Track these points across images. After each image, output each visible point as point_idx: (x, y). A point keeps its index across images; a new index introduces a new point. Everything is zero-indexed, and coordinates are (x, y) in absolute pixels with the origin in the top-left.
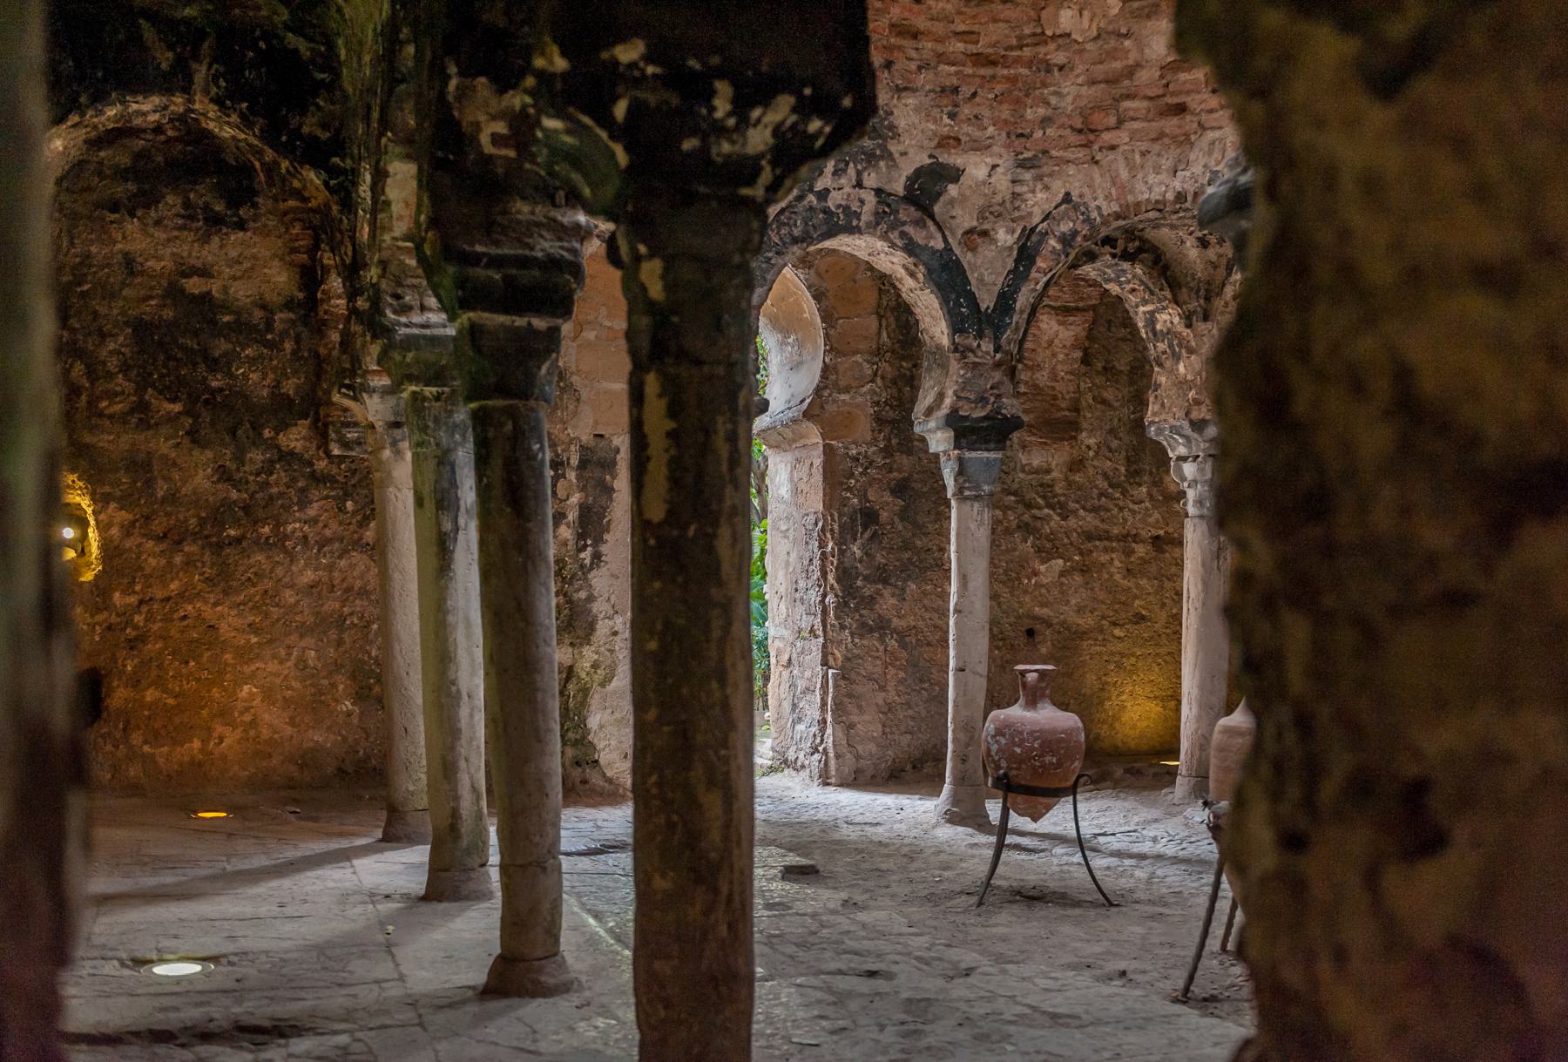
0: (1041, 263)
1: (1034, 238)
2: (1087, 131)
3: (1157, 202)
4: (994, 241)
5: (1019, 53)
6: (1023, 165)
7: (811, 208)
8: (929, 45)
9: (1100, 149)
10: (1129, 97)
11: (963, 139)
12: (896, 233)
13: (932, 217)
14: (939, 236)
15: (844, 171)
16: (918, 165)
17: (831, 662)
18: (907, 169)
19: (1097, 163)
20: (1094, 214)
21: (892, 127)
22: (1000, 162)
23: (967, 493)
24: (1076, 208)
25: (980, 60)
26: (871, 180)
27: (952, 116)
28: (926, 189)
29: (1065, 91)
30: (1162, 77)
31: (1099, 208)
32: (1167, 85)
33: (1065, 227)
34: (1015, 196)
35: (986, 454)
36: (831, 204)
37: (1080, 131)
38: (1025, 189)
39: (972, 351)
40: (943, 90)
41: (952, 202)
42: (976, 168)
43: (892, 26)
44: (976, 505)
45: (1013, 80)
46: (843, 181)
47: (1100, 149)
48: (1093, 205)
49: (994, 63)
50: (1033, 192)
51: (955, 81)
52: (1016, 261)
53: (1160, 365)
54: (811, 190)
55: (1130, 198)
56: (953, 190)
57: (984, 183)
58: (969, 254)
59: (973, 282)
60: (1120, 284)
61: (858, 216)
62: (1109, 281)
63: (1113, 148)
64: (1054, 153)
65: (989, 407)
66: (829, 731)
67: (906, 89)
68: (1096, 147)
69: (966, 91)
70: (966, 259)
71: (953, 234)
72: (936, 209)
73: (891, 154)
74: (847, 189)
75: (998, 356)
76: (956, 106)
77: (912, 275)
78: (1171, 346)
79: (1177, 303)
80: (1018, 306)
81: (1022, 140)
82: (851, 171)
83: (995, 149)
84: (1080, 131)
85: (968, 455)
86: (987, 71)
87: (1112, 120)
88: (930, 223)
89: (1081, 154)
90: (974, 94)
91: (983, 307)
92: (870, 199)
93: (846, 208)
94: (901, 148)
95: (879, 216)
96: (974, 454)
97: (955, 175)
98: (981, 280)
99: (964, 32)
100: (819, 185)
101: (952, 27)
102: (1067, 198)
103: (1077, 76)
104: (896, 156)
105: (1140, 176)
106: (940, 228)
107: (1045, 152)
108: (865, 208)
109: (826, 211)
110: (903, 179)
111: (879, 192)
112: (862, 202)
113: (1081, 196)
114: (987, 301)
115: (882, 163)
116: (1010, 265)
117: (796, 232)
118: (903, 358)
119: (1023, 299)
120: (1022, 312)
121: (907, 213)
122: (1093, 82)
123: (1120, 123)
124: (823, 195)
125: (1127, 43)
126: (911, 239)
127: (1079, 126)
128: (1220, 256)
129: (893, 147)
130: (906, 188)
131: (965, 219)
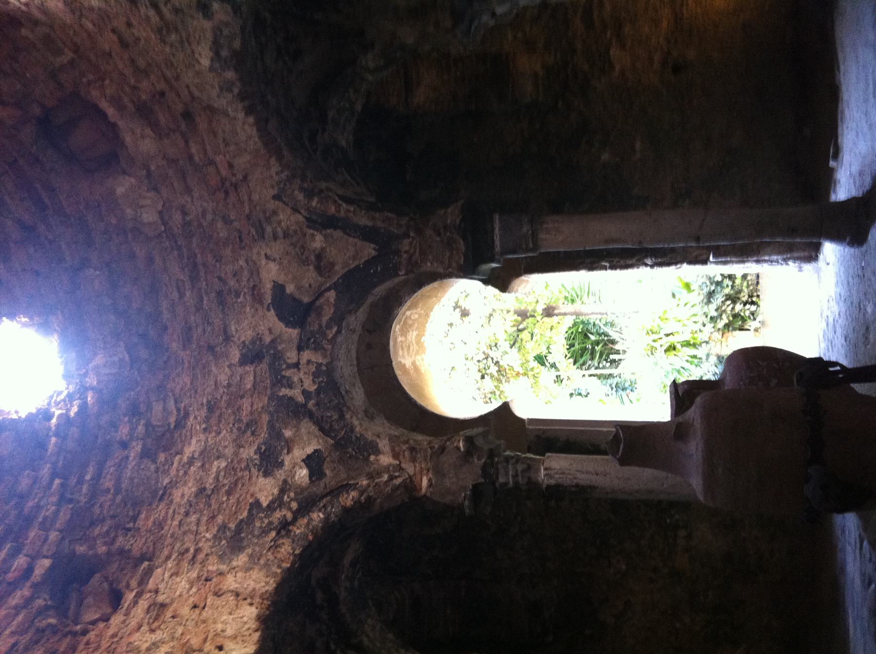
0: (333, 210)
1: (314, 217)
3: (258, 130)
4: (323, 249)
6: (262, 235)
7: (317, 404)
8: (192, 318)
9: (234, 175)
10: (191, 158)
12: (328, 332)
13: (313, 302)
14: (328, 294)
15: (289, 379)
16: (276, 319)
17: (704, 257)
18: (280, 327)
19: (245, 178)
20: (283, 176)
21: (253, 342)
22: (263, 253)
23: (531, 245)
26: (292, 356)
27: (237, 295)
29: (200, 210)
34: (286, 235)
35: (497, 231)
37: (227, 193)
38: (279, 229)
39: (411, 257)
41: (299, 288)
43: (184, 348)
44: (542, 236)
46: (296, 379)
47: (234, 175)
48: (276, 178)
49: (195, 265)
50: (279, 222)
52: (335, 228)
54: (305, 406)
55: (262, 152)
56: (290, 289)
57: (280, 264)
58: (337, 268)
59: (357, 263)
61: (319, 365)
63: (231, 166)
64: (247, 211)
65: (455, 236)
66: (767, 258)
67: (225, 332)
68: (234, 180)
70: (340, 270)
71: (322, 284)
72: (306, 300)
74: (301, 375)
75: (412, 234)
80: (369, 223)
82: (288, 373)
83: (255, 257)
84: (227, 193)
85: (498, 249)
87: (211, 169)
88: (318, 303)
89: (243, 191)
90: (220, 278)
91: (374, 253)
92: (306, 355)
94: (267, 332)
95: (317, 348)
96: (497, 242)
98: (354, 258)
99: (179, 291)
100: (301, 399)
101: (177, 300)
102: (276, 197)
103: (187, 202)
106: (320, 295)
108: (314, 359)
109: (318, 392)
110: (287, 329)
111: (300, 349)
112: (309, 362)
113: (272, 187)
114: (370, 250)
115: (280, 348)
116: (338, 234)
117: (335, 417)
119: (363, 220)
120: (373, 219)
122: (188, 190)
123: (212, 162)
124: (305, 393)
125: (153, 168)
126: (331, 319)
127: (223, 195)
129: (267, 339)
130: (294, 327)
131: (310, 276)
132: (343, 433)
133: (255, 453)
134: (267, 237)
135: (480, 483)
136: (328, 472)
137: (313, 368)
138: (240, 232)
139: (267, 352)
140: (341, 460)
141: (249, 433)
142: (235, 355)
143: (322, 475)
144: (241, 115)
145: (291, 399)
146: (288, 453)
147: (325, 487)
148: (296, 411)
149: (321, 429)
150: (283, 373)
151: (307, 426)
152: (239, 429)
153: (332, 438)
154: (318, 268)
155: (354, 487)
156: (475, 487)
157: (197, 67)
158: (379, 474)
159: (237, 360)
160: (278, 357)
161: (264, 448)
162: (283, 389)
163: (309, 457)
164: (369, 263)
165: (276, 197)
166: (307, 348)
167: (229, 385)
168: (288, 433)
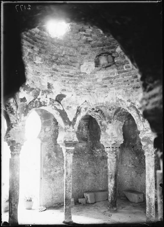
1: (80, 108)
2: (89, 89)
5: (76, 75)
6: (77, 95)
7: (37, 101)
9: (92, 93)
11: (66, 89)
13: (60, 104)
14: (62, 107)
15: (43, 95)
21: (53, 87)
24: (87, 103)
25: (69, 76)
26: (49, 96)
27: (64, 85)
28: (59, 98)
30: (102, 81)
31: (92, 103)
32: (103, 82)
33: (85, 106)
34: (76, 101)
36: (41, 101)
40: (63, 81)
41: (64, 101)
42: (68, 95)
45: (75, 80)
48: (90, 103)
49: (72, 77)
51: (65, 80)
53: (102, 130)
54: (37, 98)
55: (97, 102)
56: (64, 99)
60: (95, 116)
62: (93, 116)
68: (91, 92)
69: (67, 81)
72: (61, 102)
73: (52, 92)
74: (44, 98)
76: (65, 84)
77: (57, 114)
78: (104, 127)
79: (105, 120)
81: (77, 90)
83: (73, 92)
86: (71, 78)
88: (60, 105)
92: (49, 100)
93: (44, 102)
94: (55, 91)
97: (64, 96)
102: (86, 101)
104: (53, 92)
105: (99, 98)
106: (62, 106)
107: (82, 93)
108: (48, 102)
109: (39, 102)
111: (50, 99)
112: (47, 101)
114: (71, 120)
115: (51, 94)
116: (76, 113)
117: (34, 106)
118: (56, 127)
121: (56, 103)
126: (56, 108)
128: (113, 112)
129: (53, 90)
130: (56, 98)
132: (30, 107)
133: (27, 84)
134: (77, 96)
135: (15, 143)
136: (21, 103)
137: (46, 101)
138: (78, 90)
139: (50, 90)
140: (23, 107)
141: (32, 83)
142: (50, 82)
143: (21, 101)
144: (106, 100)
145: (39, 95)
146: (27, 93)
147: (18, 102)
148: (36, 95)
149: (31, 102)
150: (45, 94)
151: (32, 98)
152: (33, 80)
153: (28, 104)
154: (68, 107)
155: (17, 110)
156: (14, 141)
157: (117, 95)
158: (19, 116)
159: (49, 82)
160: (49, 92)
161: (28, 86)
162: (41, 93)
163: (25, 98)
164: (68, 119)
165: (86, 101)
166: (50, 101)
167: (43, 79)
168: (31, 93)
